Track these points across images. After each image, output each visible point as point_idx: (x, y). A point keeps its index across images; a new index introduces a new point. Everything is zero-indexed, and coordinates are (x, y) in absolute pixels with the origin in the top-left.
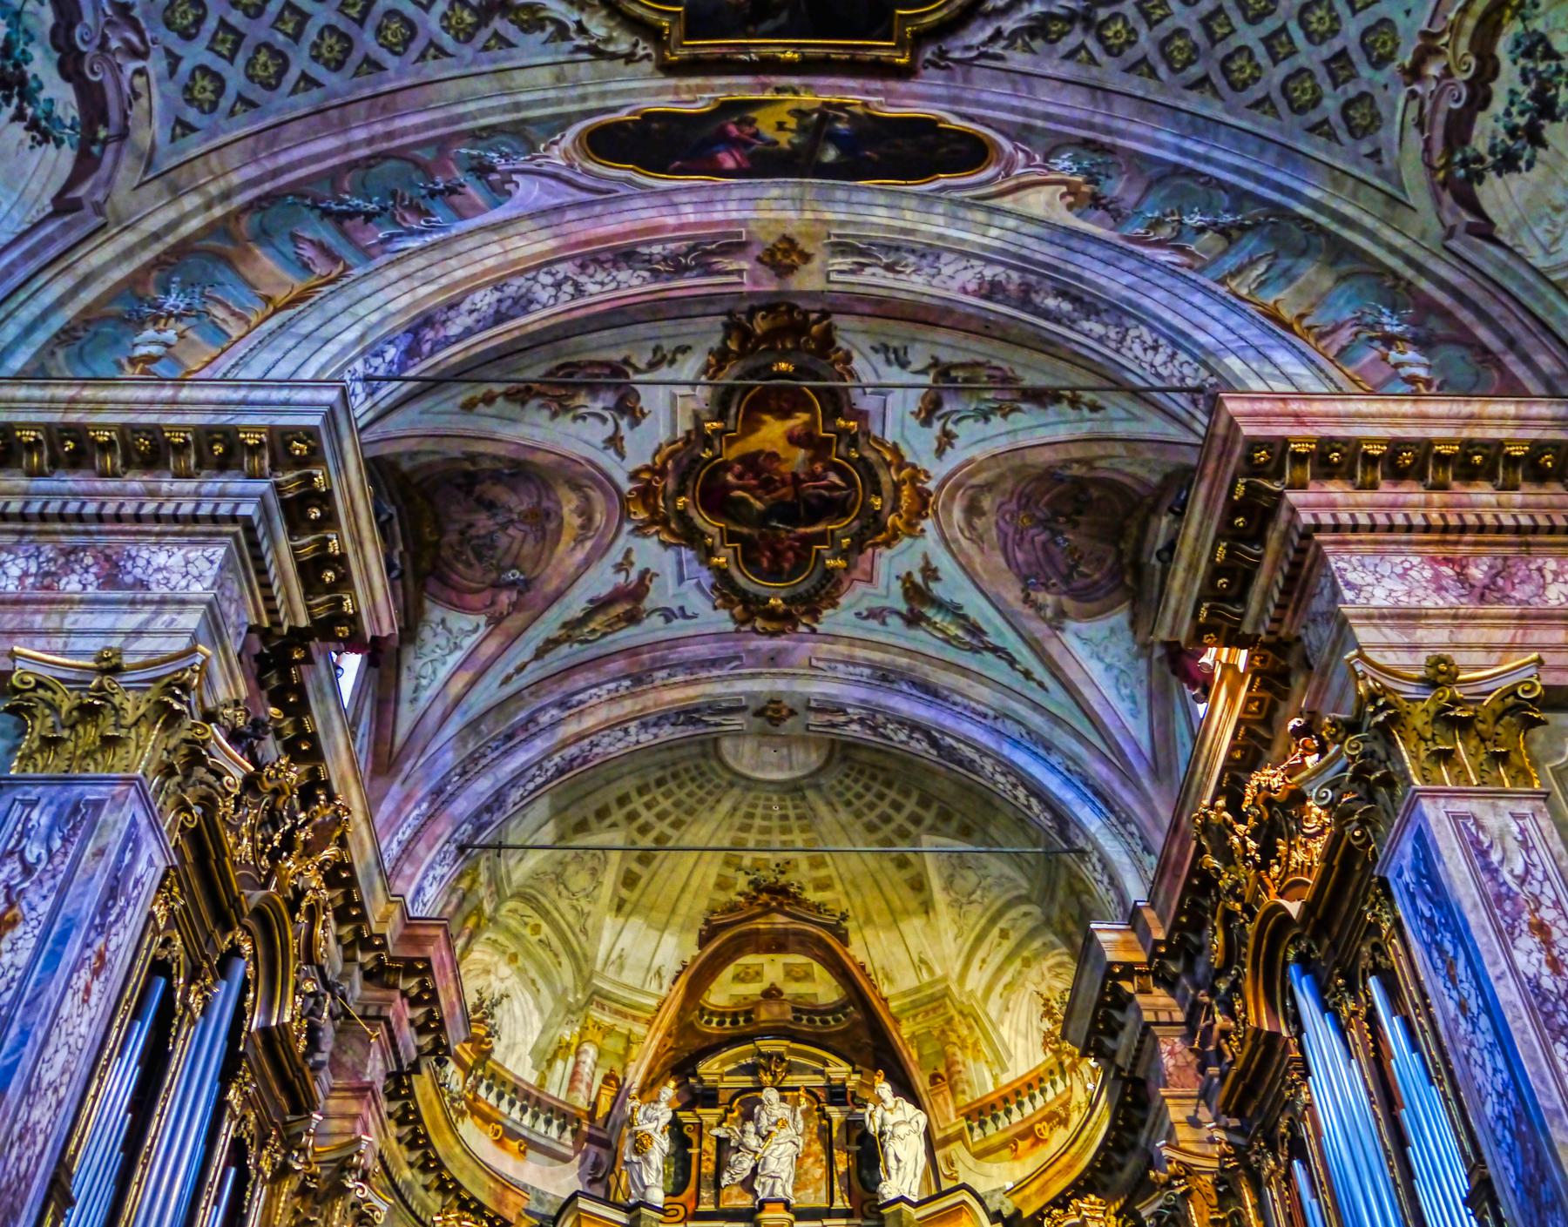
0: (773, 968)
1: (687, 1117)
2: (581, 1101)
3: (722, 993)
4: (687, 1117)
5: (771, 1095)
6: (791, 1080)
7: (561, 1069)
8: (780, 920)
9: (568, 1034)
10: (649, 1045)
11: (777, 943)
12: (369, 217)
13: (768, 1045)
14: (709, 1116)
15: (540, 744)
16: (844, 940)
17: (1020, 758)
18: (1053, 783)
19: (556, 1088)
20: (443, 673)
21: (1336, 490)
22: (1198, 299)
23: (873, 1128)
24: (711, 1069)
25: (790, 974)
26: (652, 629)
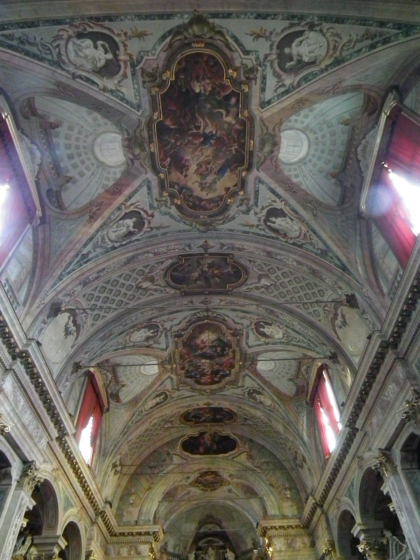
0: (210, 526)
1: (197, 552)
2: (180, 553)
3: (202, 530)
4: (197, 552)
5: (210, 549)
6: (215, 544)
7: (177, 548)
8: (211, 520)
9: (178, 543)
10: (191, 541)
11: (211, 523)
12: (155, 467)
13: (209, 538)
14: (200, 552)
15: (175, 514)
16: (221, 523)
17: (246, 513)
18: (250, 518)
19: (176, 552)
20: (163, 509)
21: (274, 530)
22: (262, 483)
23: (226, 557)
24: (200, 544)
25: (213, 527)
26: (191, 495)
